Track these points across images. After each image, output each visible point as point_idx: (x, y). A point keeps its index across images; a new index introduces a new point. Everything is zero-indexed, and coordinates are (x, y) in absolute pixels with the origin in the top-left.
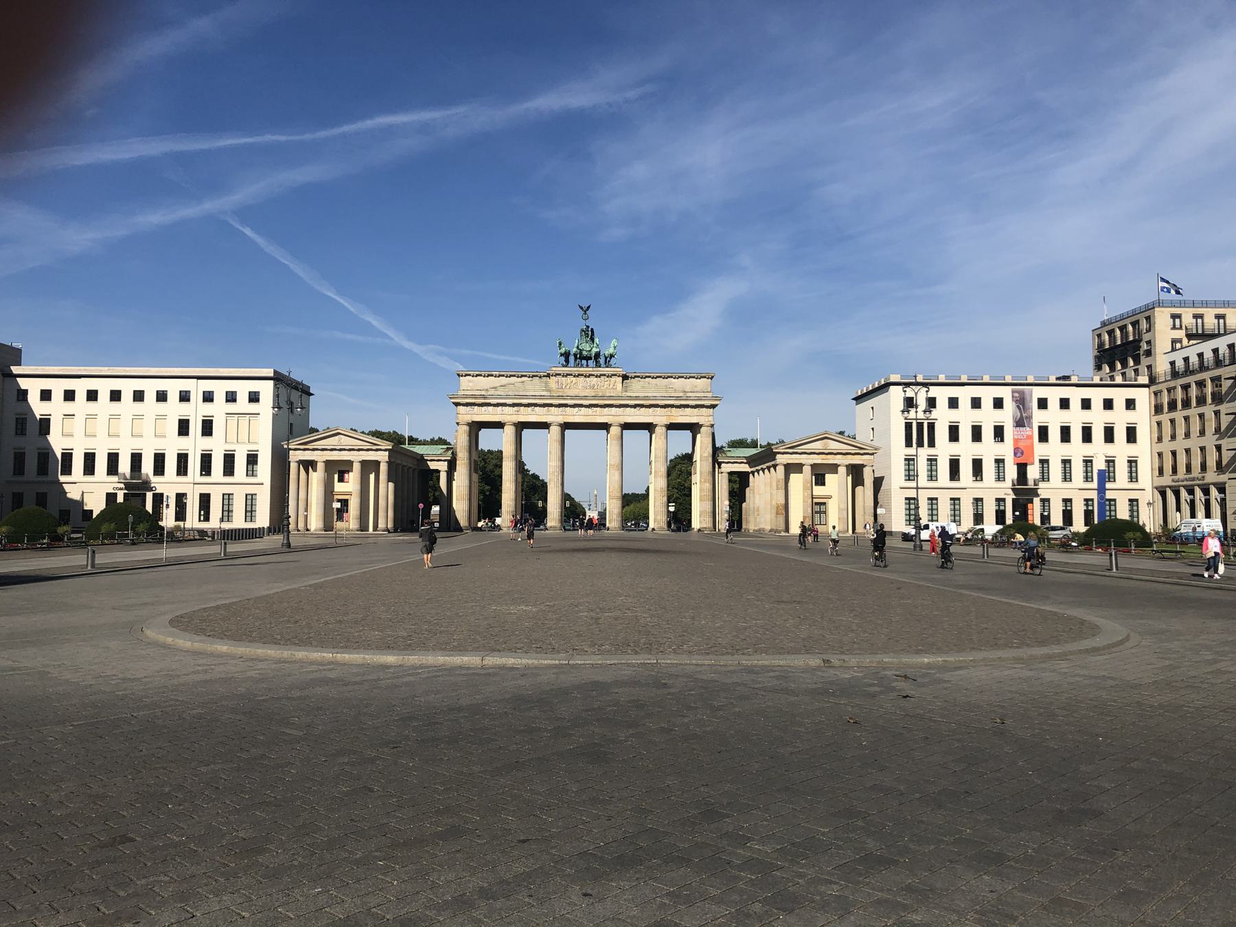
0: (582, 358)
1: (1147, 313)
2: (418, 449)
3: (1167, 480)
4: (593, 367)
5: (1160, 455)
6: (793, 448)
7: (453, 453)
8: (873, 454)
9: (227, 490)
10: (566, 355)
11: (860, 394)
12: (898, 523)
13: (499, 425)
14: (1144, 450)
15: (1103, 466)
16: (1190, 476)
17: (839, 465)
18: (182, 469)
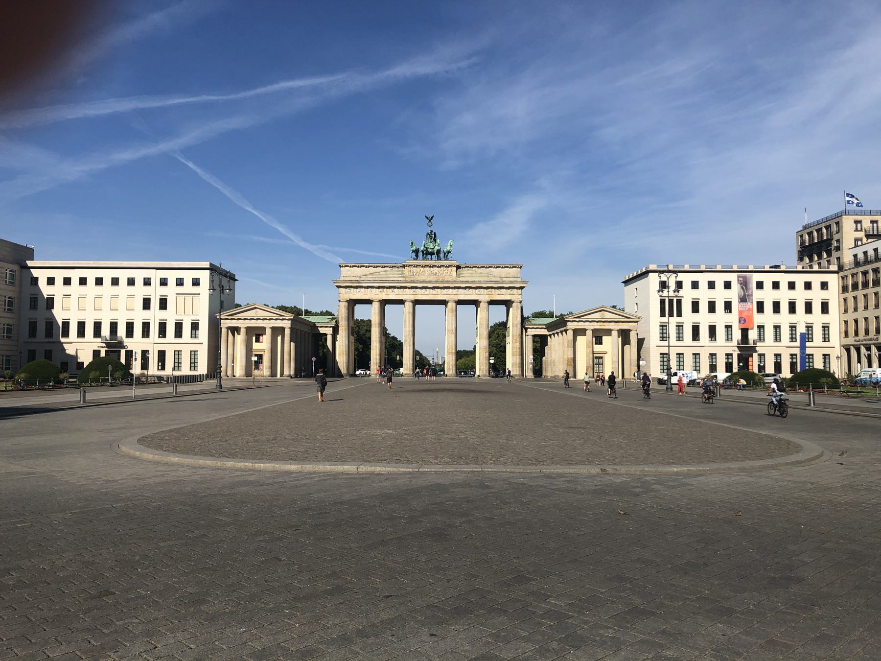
0: (428, 253)
1: (837, 220)
2: (312, 319)
3: (851, 340)
4: (435, 260)
5: (846, 322)
6: (579, 318)
7: (336, 322)
8: (637, 322)
9: (178, 348)
10: (416, 252)
11: (627, 279)
12: (655, 372)
13: (369, 302)
14: (834, 318)
15: (804, 330)
16: (868, 337)
17: (612, 330)
18: (146, 333)
